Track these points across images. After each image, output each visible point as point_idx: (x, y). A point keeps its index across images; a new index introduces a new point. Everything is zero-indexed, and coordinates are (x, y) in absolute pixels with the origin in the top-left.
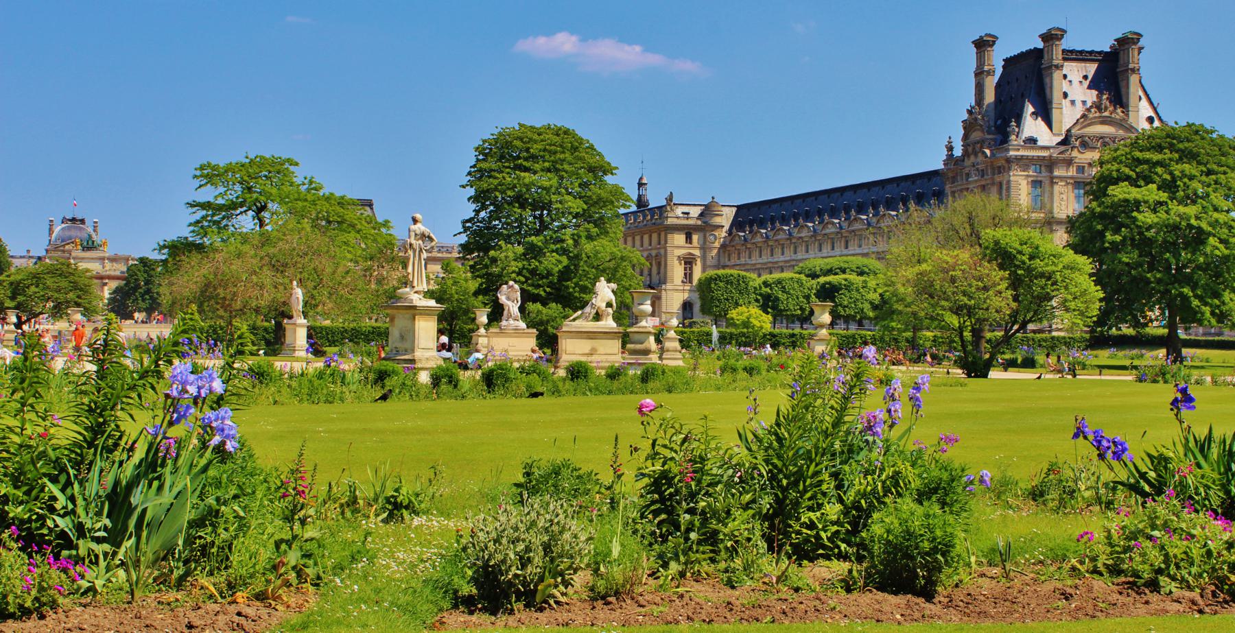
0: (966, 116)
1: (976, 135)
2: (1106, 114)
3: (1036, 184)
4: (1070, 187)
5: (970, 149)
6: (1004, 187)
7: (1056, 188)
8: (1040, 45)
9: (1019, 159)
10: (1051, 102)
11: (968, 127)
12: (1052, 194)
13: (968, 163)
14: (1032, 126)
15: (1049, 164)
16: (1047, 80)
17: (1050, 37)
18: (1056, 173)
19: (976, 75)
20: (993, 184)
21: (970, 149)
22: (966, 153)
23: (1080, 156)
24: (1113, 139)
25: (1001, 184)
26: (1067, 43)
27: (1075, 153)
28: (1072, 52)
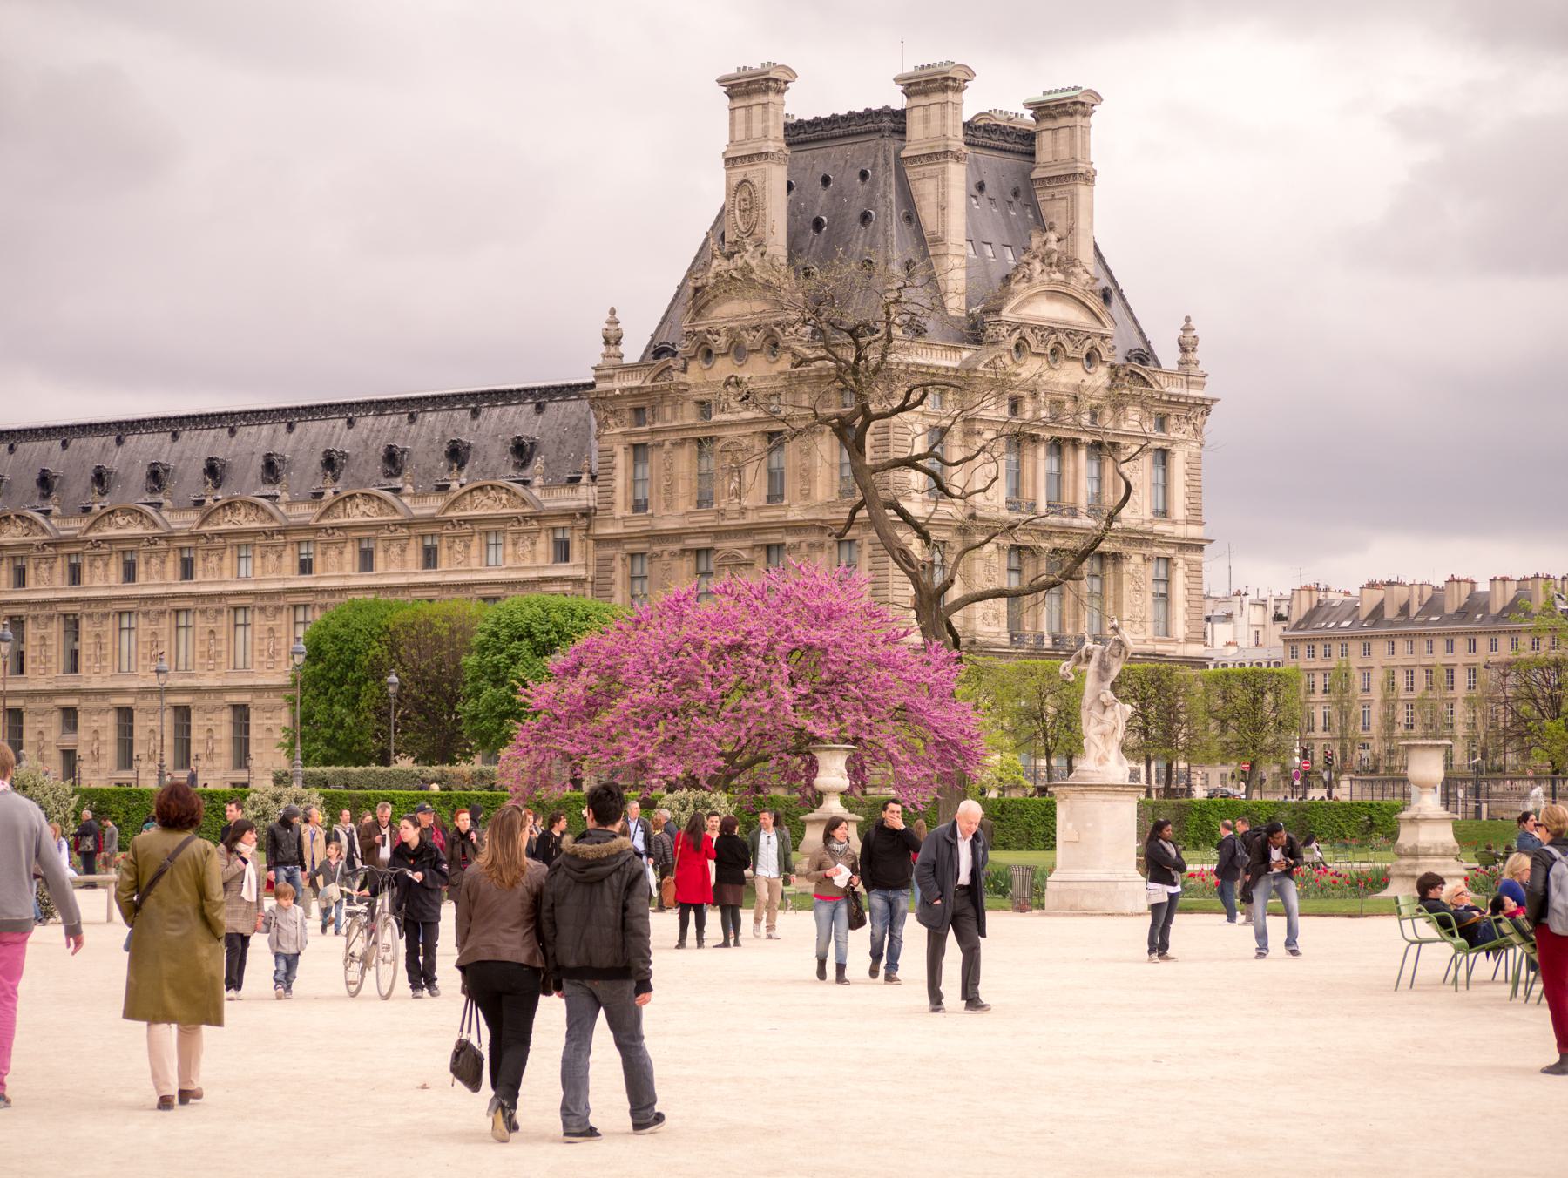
8: (898, 101)
10: (938, 241)
16: (925, 191)
17: (932, 84)
19: (730, 161)
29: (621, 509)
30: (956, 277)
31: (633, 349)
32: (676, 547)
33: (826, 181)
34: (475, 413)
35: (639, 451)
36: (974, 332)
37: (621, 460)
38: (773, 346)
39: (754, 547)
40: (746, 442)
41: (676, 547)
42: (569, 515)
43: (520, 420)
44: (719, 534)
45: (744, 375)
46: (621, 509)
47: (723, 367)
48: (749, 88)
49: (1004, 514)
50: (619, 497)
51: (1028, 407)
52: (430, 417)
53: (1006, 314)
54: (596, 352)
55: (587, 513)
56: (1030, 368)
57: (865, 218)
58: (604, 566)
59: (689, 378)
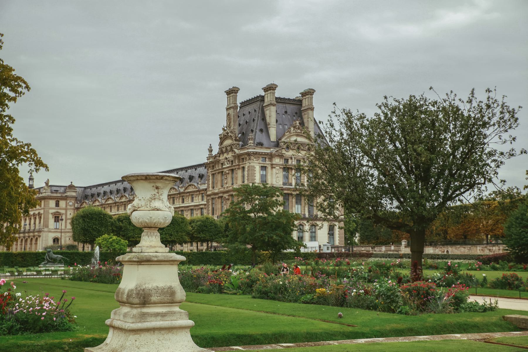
0: (221, 132)
1: (228, 142)
2: (299, 131)
3: (264, 168)
4: (281, 170)
5: (224, 150)
6: (246, 169)
7: (274, 170)
8: (263, 93)
9: (256, 153)
10: (269, 124)
11: (223, 138)
12: (272, 174)
13: (222, 158)
14: (260, 137)
15: (271, 156)
16: (267, 113)
18: (274, 162)
20: (239, 169)
21: (224, 150)
22: (221, 152)
23: (287, 153)
24: (302, 144)
25: (243, 168)
26: (278, 93)
27: (284, 151)
28: (280, 98)
29: (211, 189)
30: (273, 132)
31: (215, 152)
32: (217, 196)
33: (249, 112)
34: (196, 169)
35: (213, 175)
36: (277, 144)
37: (211, 178)
38: (232, 150)
39: (229, 196)
40: (227, 172)
41: (217, 196)
42: (203, 190)
43: (202, 170)
44: (224, 193)
45: (227, 157)
46: (211, 189)
47: (225, 155)
48: (232, 92)
49: (282, 186)
50: (210, 186)
51: (290, 161)
52: (189, 171)
53: (283, 140)
54: (207, 154)
55: (206, 190)
56: (290, 153)
57: (254, 120)
58: (208, 201)
59: (220, 158)
